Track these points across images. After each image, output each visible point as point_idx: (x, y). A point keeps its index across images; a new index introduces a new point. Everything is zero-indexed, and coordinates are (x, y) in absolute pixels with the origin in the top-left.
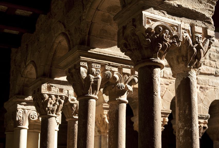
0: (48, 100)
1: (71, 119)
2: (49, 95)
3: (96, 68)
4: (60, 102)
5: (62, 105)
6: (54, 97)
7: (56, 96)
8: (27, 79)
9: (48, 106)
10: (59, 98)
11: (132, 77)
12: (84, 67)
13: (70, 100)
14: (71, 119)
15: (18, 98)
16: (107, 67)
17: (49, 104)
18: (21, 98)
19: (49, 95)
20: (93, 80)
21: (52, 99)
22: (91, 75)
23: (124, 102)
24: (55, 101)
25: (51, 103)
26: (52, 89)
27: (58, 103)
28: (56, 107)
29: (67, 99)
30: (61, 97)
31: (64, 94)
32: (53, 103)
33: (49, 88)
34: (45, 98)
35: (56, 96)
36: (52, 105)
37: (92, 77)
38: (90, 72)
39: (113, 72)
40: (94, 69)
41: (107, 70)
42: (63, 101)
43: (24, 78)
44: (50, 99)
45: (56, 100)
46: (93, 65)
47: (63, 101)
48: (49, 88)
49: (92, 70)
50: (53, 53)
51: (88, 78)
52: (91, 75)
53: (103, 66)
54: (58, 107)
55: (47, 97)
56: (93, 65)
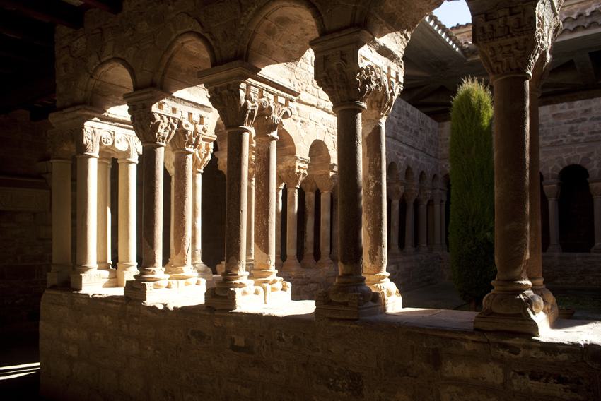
0: (159, 122)
1: (181, 151)
2: (160, 115)
3: (254, 93)
4: (172, 127)
5: (174, 132)
6: (165, 117)
7: (169, 118)
8: (99, 83)
9: (159, 131)
10: (172, 121)
11: (286, 109)
12: (243, 89)
13: (183, 125)
14: (181, 151)
15: (86, 109)
16: (265, 93)
17: (160, 127)
18: (90, 111)
19: (160, 115)
20: (250, 108)
21: (164, 122)
22: (248, 101)
23: (273, 139)
24: (166, 125)
25: (162, 128)
26: (164, 108)
27: (169, 127)
28: (167, 133)
29: (180, 123)
30: (174, 119)
31: (178, 116)
32: (164, 127)
33: (160, 107)
34: (155, 120)
35: (169, 118)
36: (163, 130)
37: (250, 104)
38: (248, 97)
39: (268, 99)
40: (252, 95)
41: (264, 97)
42: (176, 126)
43: (94, 81)
44: (162, 121)
45: (168, 123)
46: (252, 88)
47: (176, 126)
48: (160, 107)
49: (250, 96)
50: (168, 56)
51: (246, 104)
52: (248, 101)
53: (261, 90)
54: (170, 133)
55: (158, 118)
56: (252, 88)
